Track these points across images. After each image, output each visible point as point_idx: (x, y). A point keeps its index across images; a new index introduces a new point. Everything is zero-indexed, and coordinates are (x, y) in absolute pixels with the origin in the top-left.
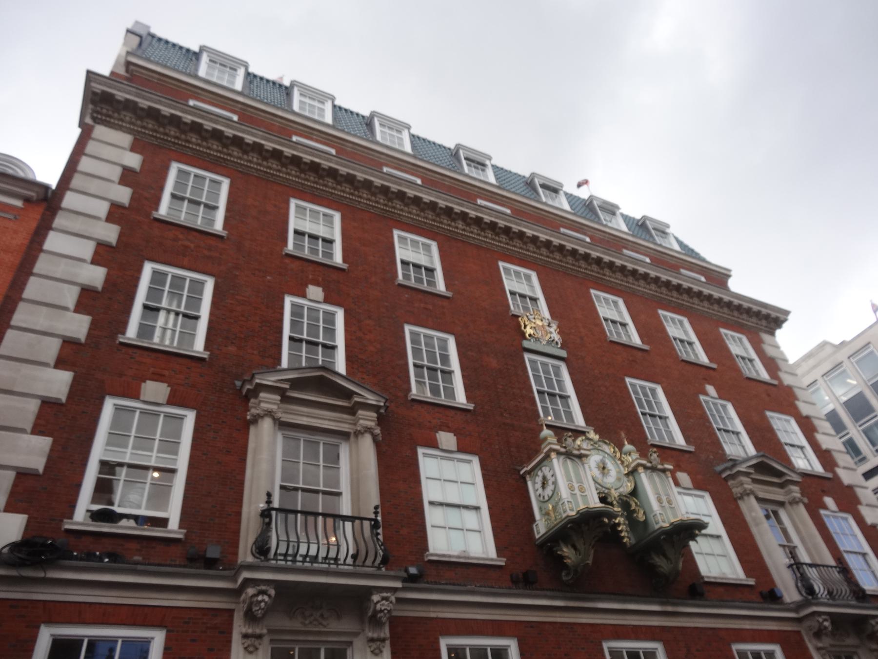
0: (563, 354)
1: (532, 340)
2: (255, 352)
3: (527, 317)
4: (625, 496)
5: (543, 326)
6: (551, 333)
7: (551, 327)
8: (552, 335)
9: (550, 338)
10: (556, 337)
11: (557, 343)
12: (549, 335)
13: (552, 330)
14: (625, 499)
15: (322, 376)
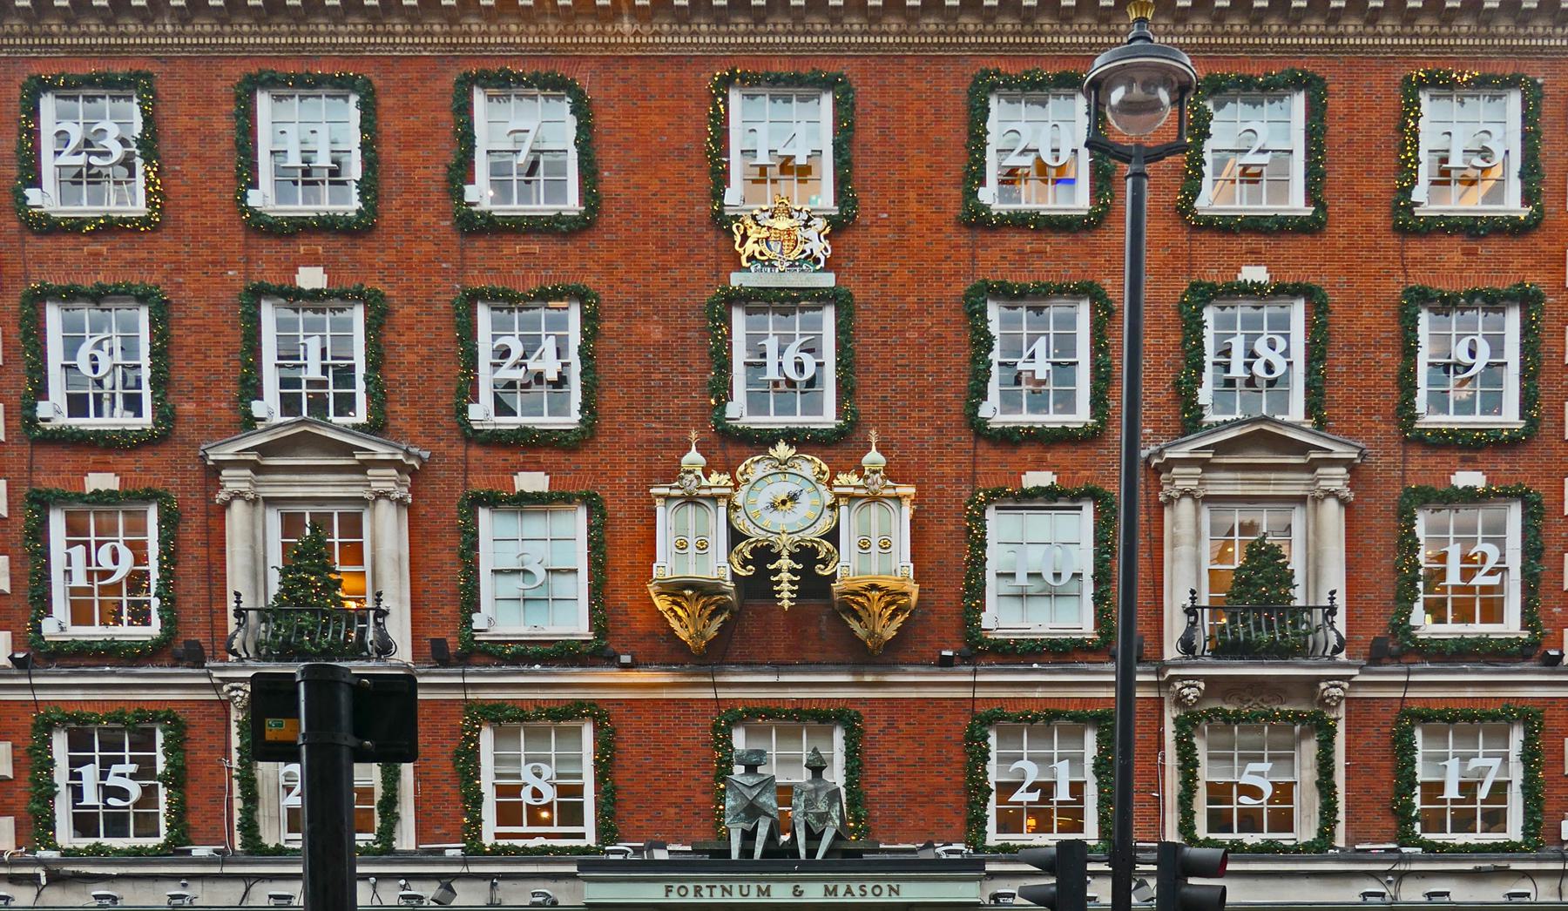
0: (828, 280)
1: (752, 269)
2: (224, 405)
3: (754, 217)
4: (811, 541)
5: (789, 232)
6: (807, 241)
7: (810, 226)
8: (807, 247)
9: (804, 251)
10: (820, 248)
11: (817, 261)
12: (800, 247)
13: (812, 233)
14: (809, 545)
15: (305, 431)
